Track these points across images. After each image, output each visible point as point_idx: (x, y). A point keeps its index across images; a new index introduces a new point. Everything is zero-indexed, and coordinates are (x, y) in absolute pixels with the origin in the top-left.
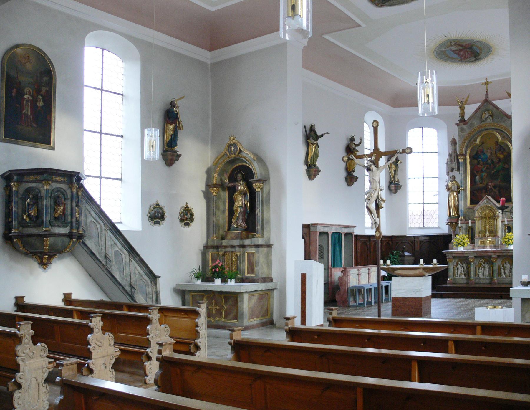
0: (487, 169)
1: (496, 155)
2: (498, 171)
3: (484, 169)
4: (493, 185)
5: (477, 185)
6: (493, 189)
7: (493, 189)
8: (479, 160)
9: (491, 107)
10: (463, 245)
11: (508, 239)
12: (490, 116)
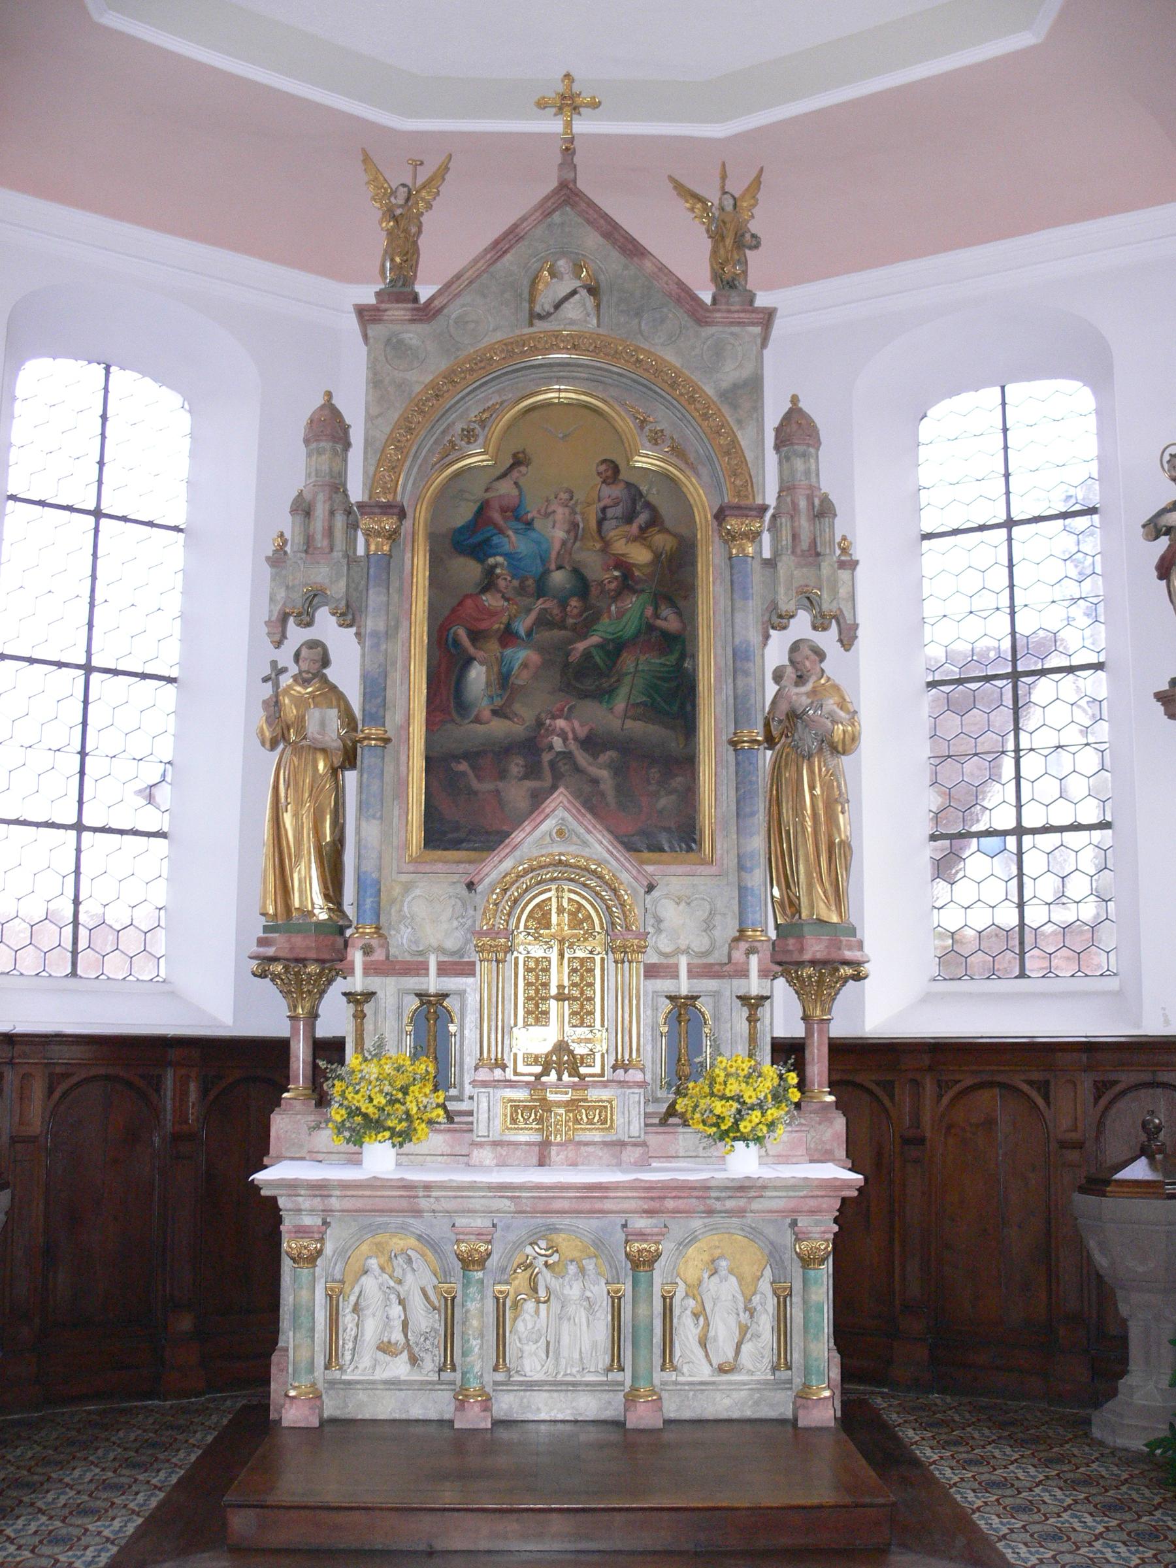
0: (543, 621)
1: (606, 545)
2: (615, 649)
3: (521, 627)
4: (582, 732)
5: (477, 720)
6: (582, 758)
7: (582, 758)
8: (491, 561)
9: (592, 241)
10: (402, 1137)
11: (738, 1098)
12: (584, 292)
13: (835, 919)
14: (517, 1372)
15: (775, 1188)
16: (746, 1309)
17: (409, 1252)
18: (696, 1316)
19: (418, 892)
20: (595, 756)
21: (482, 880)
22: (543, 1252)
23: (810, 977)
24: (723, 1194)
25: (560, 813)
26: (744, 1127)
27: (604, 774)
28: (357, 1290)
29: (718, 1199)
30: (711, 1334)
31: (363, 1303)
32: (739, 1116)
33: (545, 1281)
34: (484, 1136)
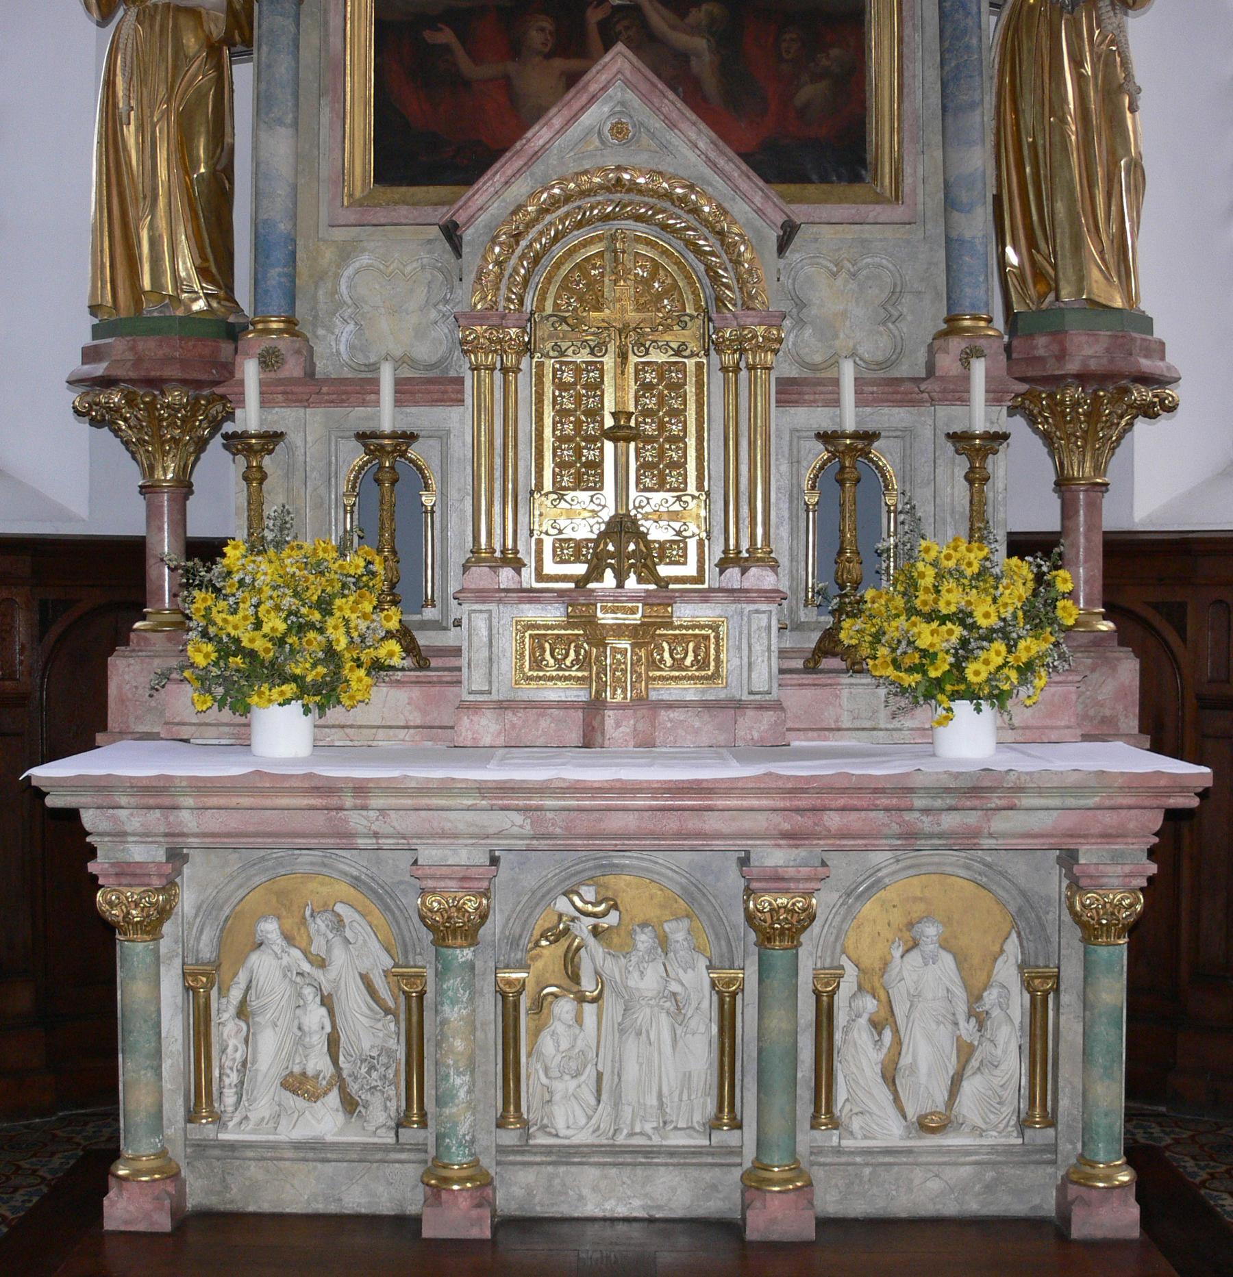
11: (963, 617)
13: (1118, 303)
14: (543, 1128)
15: (1041, 791)
16: (971, 1014)
17: (339, 908)
18: (876, 1026)
19: (365, 259)
20: (682, 13)
21: (471, 219)
22: (590, 908)
23: (1076, 404)
24: (938, 803)
25: (617, 92)
26: (976, 672)
27: (700, 44)
28: (242, 977)
29: (926, 811)
30: (905, 1060)
31: (254, 1003)
32: (964, 652)
33: (593, 960)
34: (482, 693)
